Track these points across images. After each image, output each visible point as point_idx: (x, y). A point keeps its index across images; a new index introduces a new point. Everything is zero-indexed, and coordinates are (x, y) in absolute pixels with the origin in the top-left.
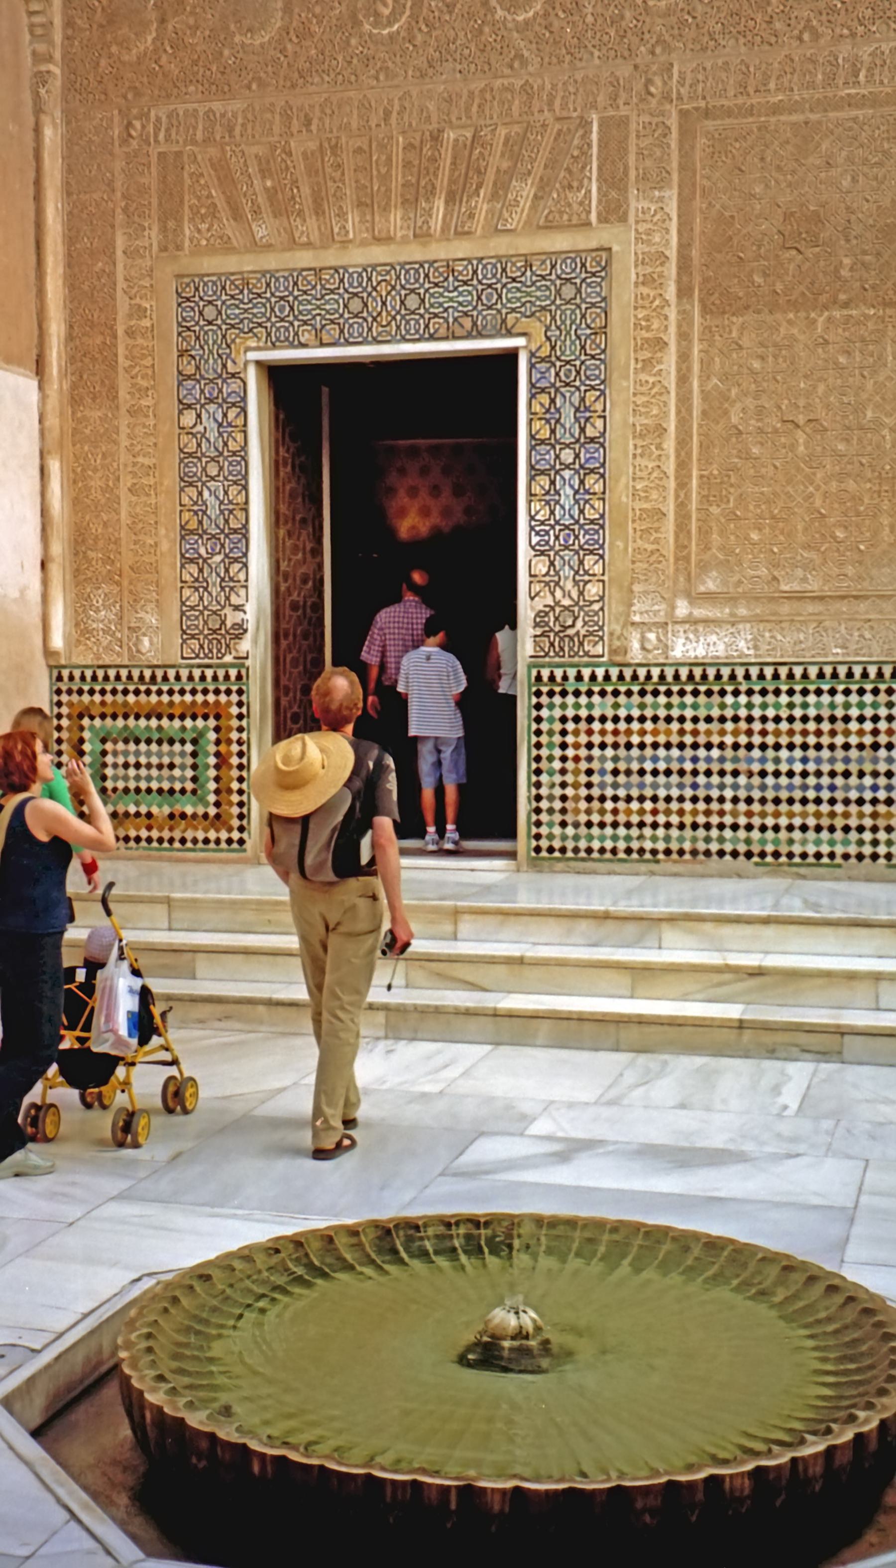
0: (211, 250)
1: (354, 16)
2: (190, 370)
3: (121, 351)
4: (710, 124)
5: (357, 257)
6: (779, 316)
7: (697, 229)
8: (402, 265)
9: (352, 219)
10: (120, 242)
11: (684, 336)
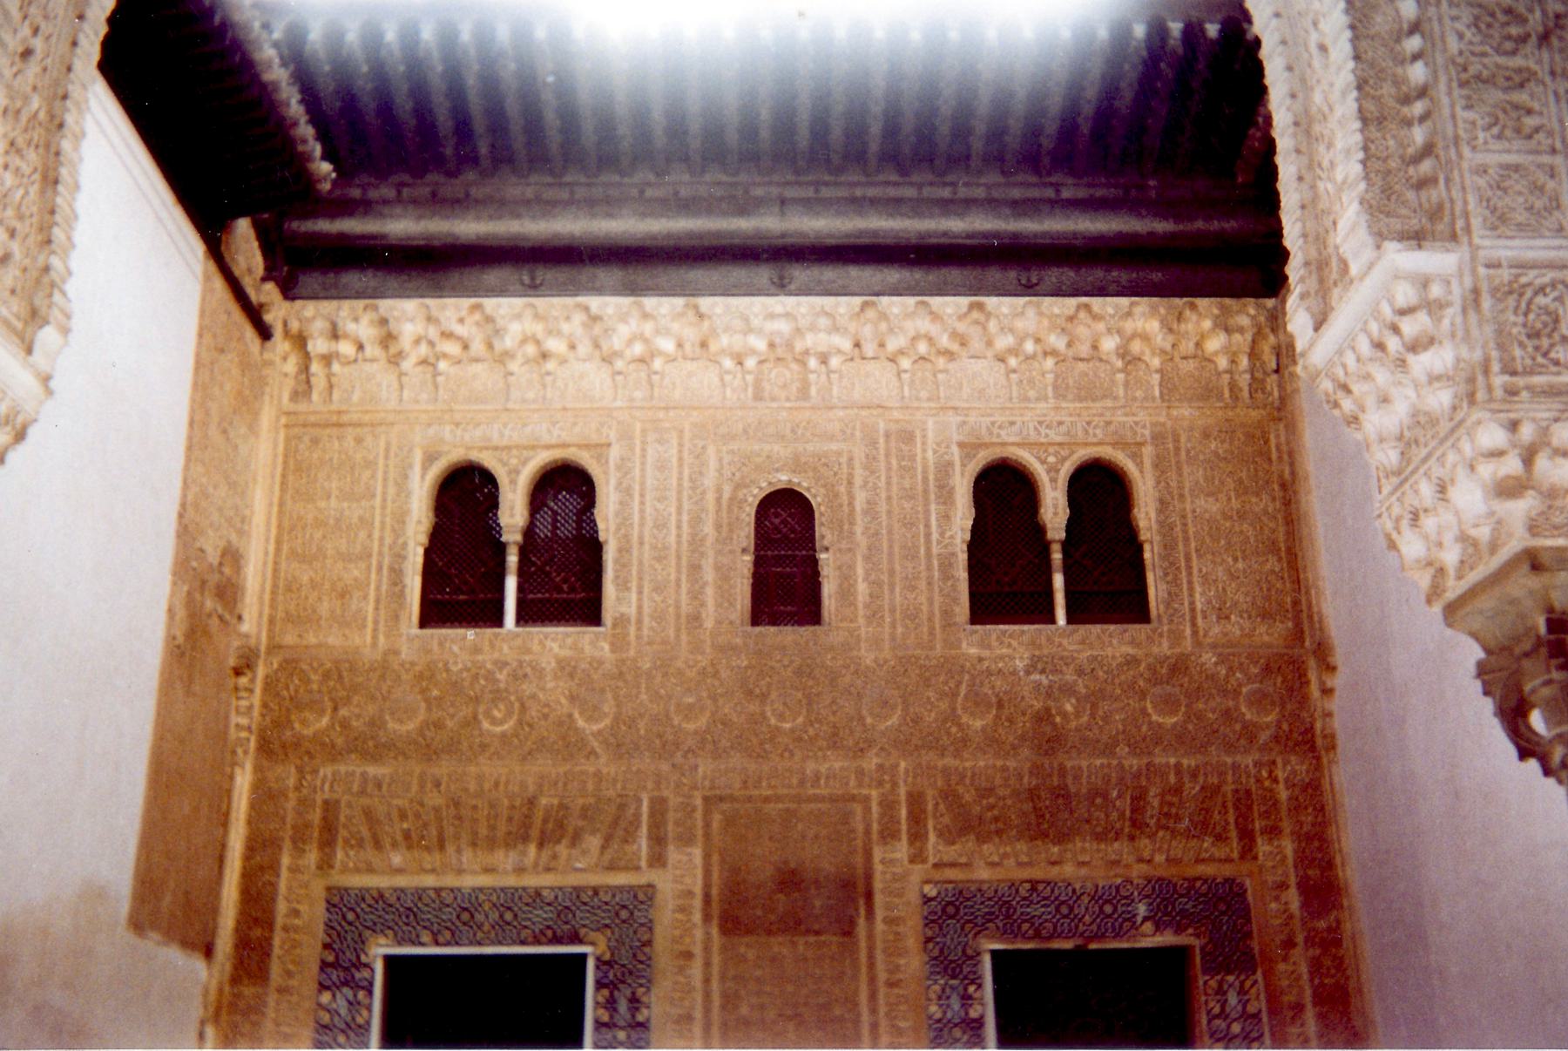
0: (357, 870)
1: (475, 717)
2: (331, 958)
3: (277, 942)
4: (725, 806)
5: (469, 882)
6: (772, 939)
7: (715, 876)
8: (502, 889)
9: (467, 855)
10: (286, 860)
11: (707, 949)
